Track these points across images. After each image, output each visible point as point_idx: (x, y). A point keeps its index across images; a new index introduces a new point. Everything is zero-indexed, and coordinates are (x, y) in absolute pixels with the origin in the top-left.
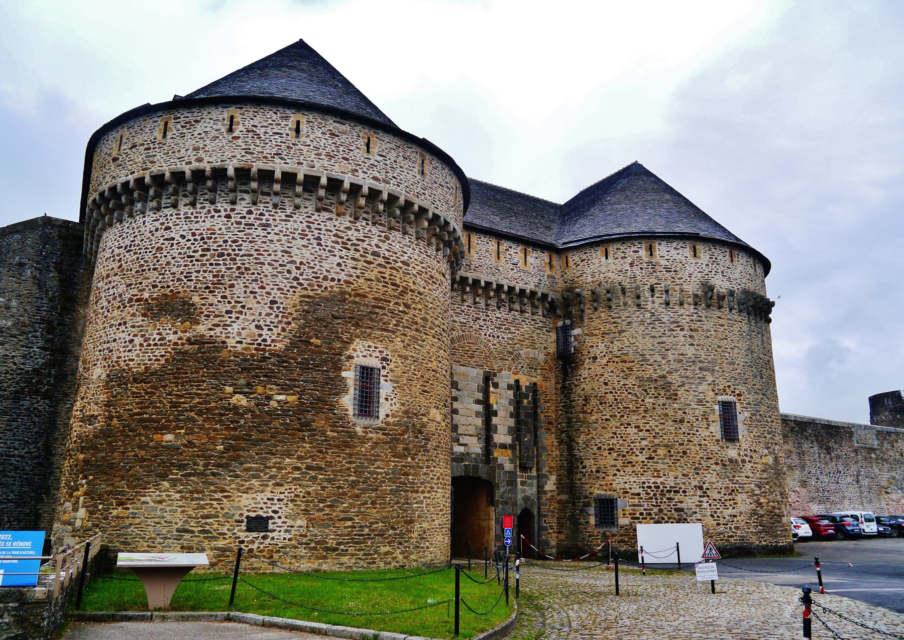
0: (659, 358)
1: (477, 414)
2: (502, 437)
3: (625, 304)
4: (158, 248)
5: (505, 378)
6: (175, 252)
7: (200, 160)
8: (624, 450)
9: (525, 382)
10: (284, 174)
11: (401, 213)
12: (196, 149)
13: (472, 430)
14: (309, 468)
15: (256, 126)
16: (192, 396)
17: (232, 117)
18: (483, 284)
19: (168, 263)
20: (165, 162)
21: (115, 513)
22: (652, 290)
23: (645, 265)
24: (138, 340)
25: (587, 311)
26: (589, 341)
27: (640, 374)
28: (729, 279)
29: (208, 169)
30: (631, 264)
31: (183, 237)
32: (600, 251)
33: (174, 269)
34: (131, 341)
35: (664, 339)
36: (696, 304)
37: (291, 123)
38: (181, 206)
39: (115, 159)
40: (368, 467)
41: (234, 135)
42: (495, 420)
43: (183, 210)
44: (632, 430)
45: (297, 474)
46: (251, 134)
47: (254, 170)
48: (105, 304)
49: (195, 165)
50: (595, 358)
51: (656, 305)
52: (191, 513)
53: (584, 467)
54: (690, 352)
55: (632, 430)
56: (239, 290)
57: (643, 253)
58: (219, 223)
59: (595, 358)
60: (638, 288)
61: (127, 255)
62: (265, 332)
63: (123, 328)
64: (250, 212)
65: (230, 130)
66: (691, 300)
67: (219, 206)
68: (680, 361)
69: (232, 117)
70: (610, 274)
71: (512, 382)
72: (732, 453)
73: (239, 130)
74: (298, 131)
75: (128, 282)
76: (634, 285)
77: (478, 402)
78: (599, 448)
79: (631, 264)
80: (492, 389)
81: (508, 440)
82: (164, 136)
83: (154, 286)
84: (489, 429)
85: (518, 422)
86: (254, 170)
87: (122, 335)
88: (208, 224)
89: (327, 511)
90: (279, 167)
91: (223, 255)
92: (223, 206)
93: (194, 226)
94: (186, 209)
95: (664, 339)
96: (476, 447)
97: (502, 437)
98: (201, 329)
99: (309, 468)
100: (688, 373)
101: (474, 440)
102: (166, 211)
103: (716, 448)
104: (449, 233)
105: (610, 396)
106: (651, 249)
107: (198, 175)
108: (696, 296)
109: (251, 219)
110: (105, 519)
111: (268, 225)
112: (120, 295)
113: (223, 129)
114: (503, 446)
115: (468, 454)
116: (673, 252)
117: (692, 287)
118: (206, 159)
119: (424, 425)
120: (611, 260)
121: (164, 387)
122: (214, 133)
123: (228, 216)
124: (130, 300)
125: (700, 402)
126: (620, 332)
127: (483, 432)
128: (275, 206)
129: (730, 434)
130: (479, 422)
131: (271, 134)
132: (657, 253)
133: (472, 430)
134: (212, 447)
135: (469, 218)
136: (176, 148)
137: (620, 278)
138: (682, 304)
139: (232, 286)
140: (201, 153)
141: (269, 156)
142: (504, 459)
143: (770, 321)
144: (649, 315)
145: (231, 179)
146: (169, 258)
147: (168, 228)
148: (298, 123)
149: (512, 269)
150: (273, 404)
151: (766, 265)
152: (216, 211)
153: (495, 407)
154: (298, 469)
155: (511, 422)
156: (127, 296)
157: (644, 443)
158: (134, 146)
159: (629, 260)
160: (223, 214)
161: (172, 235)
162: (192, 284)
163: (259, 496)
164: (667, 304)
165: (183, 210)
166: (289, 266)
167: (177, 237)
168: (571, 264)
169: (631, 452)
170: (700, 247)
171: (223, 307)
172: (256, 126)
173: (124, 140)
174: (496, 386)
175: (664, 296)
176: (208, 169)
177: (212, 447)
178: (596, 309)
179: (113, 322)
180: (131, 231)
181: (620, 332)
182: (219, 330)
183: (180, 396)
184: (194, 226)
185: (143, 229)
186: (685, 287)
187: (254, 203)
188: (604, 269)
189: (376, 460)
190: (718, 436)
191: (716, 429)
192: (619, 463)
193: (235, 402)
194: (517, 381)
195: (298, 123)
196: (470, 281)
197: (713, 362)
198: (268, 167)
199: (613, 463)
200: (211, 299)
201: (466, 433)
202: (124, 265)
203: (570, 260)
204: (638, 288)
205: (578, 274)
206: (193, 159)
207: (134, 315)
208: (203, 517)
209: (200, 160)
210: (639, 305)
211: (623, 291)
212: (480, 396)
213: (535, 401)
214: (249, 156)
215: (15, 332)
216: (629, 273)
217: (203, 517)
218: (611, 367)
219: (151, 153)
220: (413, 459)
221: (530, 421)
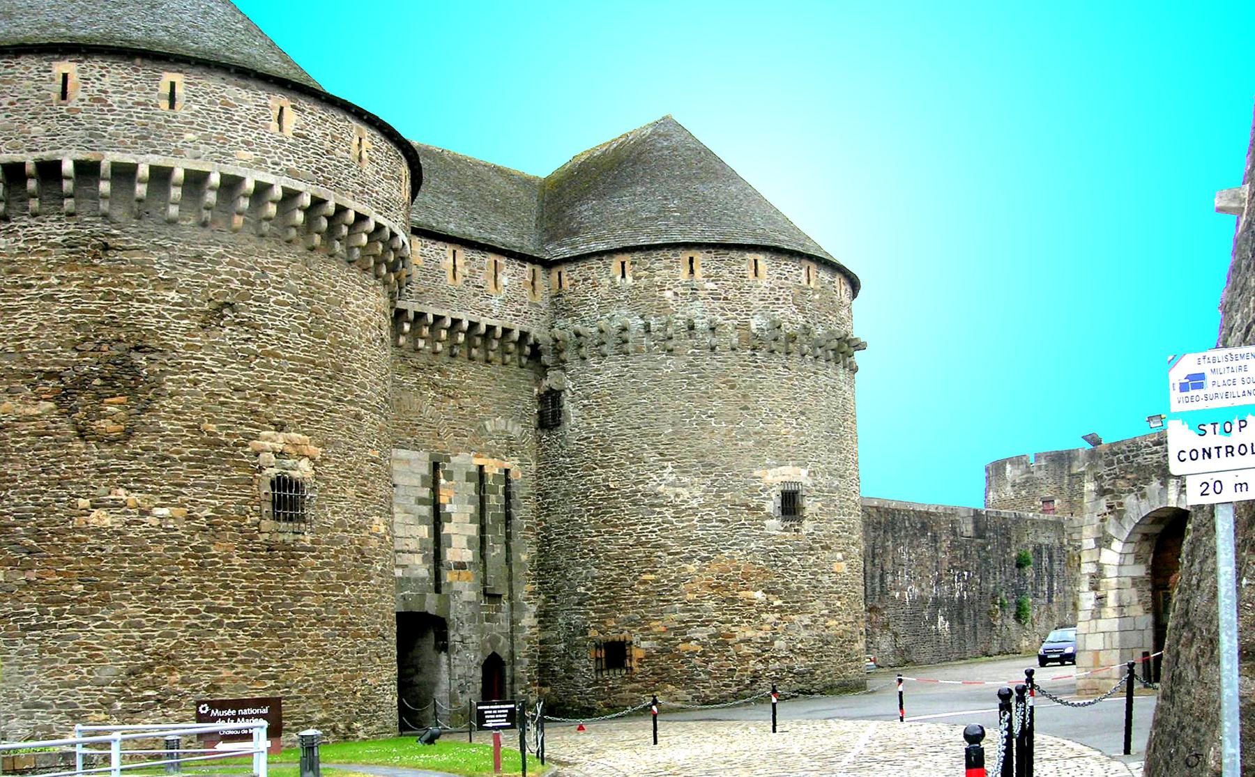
1: (422, 520)
2: (459, 550)
5: (464, 461)
9: (493, 468)
10: (153, 169)
11: (326, 226)
13: (414, 545)
14: (210, 609)
15: (105, 92)
18: (430, 319)
40: (291, 605)
41: (70, 106)
42: (448, 528)
46: (97, 106)
71: (474, 469)
77: (421, 501)
80: (443, 481)
81: (468, 556)
84: (438, 542)
85: (483, 529)
89: (240, 668)
96: (420, 568)
97: (459, 550)
99: (210, 609)
101: (417, 559)
104: (395, 250)
114: (461, 566)
115: (408, 579)
119: (364, 542)
127: (431, 546)
130: (424, 531)
131: (130, 104)
133: (414, 545)
134: (65, 587)
135: (418, 218)
141: (128, 141)
142: (464, 588)
145: (68, 178)
149: (475, 295)
151: (854, 284)
153: (448, 508)
154: (196, 612)
155: (473, 530)
172: (105, 92)
174: (449, 476)
177: (65, 587)
189: (302, 595)
193: (95, 520)
194: (481, 467)
196: (411, 316)
198: (128, 159)
201: (406, 548)
203: (564, 277)
212: (426, 493)
213: (508, 495)
220: (352, 590)
221: (501, 526)
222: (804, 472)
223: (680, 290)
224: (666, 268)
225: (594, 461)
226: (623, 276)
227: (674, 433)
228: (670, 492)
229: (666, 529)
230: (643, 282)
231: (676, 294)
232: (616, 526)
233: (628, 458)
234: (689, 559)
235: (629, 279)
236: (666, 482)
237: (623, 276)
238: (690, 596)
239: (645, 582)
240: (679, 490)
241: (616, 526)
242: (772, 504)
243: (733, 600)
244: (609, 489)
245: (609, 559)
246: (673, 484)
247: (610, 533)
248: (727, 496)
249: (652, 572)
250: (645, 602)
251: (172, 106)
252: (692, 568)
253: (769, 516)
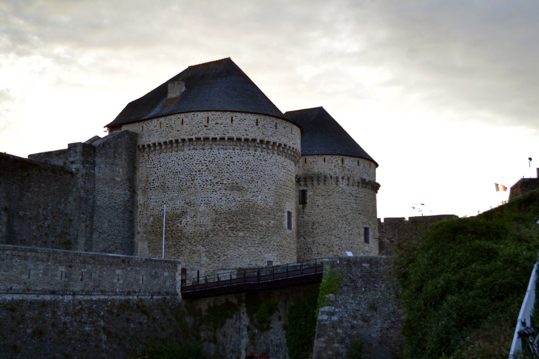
0: (344, 208)
3: (331, 183)
4: (228, 165)
6: (235, 167)
7: (247, 135)
8: (330, 245)
12: (245, 130)
16: (248, 220)
17: (257, 120)
19: (233, 171)
20: (234, 133)
21: (223, 259)
22: (343, 178)
23: (340, 167)
24: (224, 198)
25: (315, 185)
26: (316, 198)
27: (336, 214)
28: (369, 176)
29: (250, 139)
30: (335, 166)
31: (238, 162)
32: (322, 157)
33: (236, 174)
34: (220, 199)
35: (346, 200)
36: (358, 186)
37: (274, 123)
38: (235, 150)
39: (205, 126)
43: (237, 151)
44: (333, 237)
45: (277, 248)
47: (265, 141)
48: (201, 182)
49: (246, 136)
50: (318, 206)
51: (344, 185)
52: (251, 259)
53: (312, 252)
54: (355, 206)
55: (333, 237)
56: (259, 184)
57: (340, 162)
58: (251, 158)
59: (318, 206)
60: (337, 177)
61: (211, 165)
62: (267, 199)
63: (214, 193)
64: (260, 155)
65: (257, 125)
66: (356, 184)
67: (250, 152)
68: (352, 210)
69: (257, 120)
70: (325, 170)
72: (367, 248)
73: (260, 125)
74: (276, 126)
75: (214, 176)
76: (336, 176)
78: (319, 244)
79: (335, 166)
82: (232, 122)
83: (228, 179)
86: (265, 141)
87: (214, 196)
88: (247, 158)
90: (272, 140)
91: (253, 170)
92: (252, 152)
93: (242, 158)
94: (238, 151)
95: (346, 200)
98: (249, 196)
100: (355, 215)
102: (229, 150)
103: (362, 246)
105: (324, 223)
106: (343, 161)
107: (247, 140)
108: (358, 183)
109: (261, 157)
110: (218, 260)
111: (266, 160)
112: (211, 180)
113: (255, 124)
116: (351, 163)
117: (357, 179)
118: (250, 135)
120: (326, 163)
121: (237, 216)
122: (252, 125)
123: (254, 156)
124: (217, 183)
125: (358, 227)
126: (329, 195)
128: (268, 153)
129: (367, 240)
132: (345, 163)
136: (238, 129)
137: (330, 172)
138: (353, 186)
139: (257, 182)
140: (248, 133)
143: (377, 192)
144: (341, 189)
146: (233, 169)
147: (231, 158)
148: (276, 123)
150: (271, 224)
152: (250, 153)
156: (215, 181)
157: (338, 243)
158: (217, 124)
159: (334, 164)
160: (252, 155)
161: (233, 160)
162: (244, 180)
163: (270, 254)
164: (348, 185)
165: (237, 151)
166: (272, 176)
167: (236, 162)
168: (308, 161)
169: (332, 246)
170: (361, 160)
171: (256, 190)
173: (210, 119)
175: (347, 182)
176: (250, 139)
178: (319, 184)
179: (208, 190)
180: (211, 155)
181: (329, 195)
182: (254, 198)
183: (243, 220)
184: (242, 158)
185: (219, 156)
186: (355, 179)
187: (262, 152)
188: (323, 167)
190: (363, 241)
191: (362, 238)
192: (327, 251)
195: (276, 123)
197: (363, 211)
198: (269, 140)
199: (324, 250)
200: (251, 186)
202: (210, 168)
203: (307, 160)
204: (337, 177)
205: (311, 167)
206: (245, 134)
207: (220, 189)
208: (256, 260)
209: (247, 135)
210: (337, 185)
211: (331, 177)
214: (263, 136)
215: (122, 183)
216: (334, 170)
217: (256, 260)
218: (325, 210)
219: (227, 128)
251: (276, 128)
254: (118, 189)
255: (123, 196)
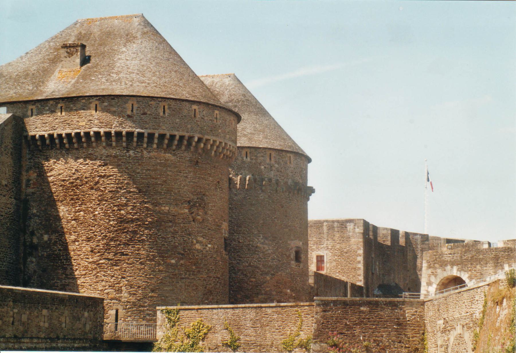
222: (301, 243)
223: (267, 166)
224: (262, 156)
225: (234, 230)
226: (247, 157)
227: (263, 223)
228: (261, 246)
229: (260, 261)
230: (254, 161)
231: (265, 167)
232: (242, 257)
233: (247, 231)
234: (267, 274)
235: (249, 159)
236: (259, 242)
237: (247, 157)
238: (268, 289)
239: (252, 282)
240: (265, 246)
241: (242, 257)
242: (293, 256)
243: (281, 292)
244: (239, 242)
245: (239, 270)
246: (263, 243)
247: (240, 260)
248: (280, 250)
249: (254, 278)
250: (252, 289)
252: (268, 278)
253: (292, 260)
254: (4, 196)
255: (9, 206)
